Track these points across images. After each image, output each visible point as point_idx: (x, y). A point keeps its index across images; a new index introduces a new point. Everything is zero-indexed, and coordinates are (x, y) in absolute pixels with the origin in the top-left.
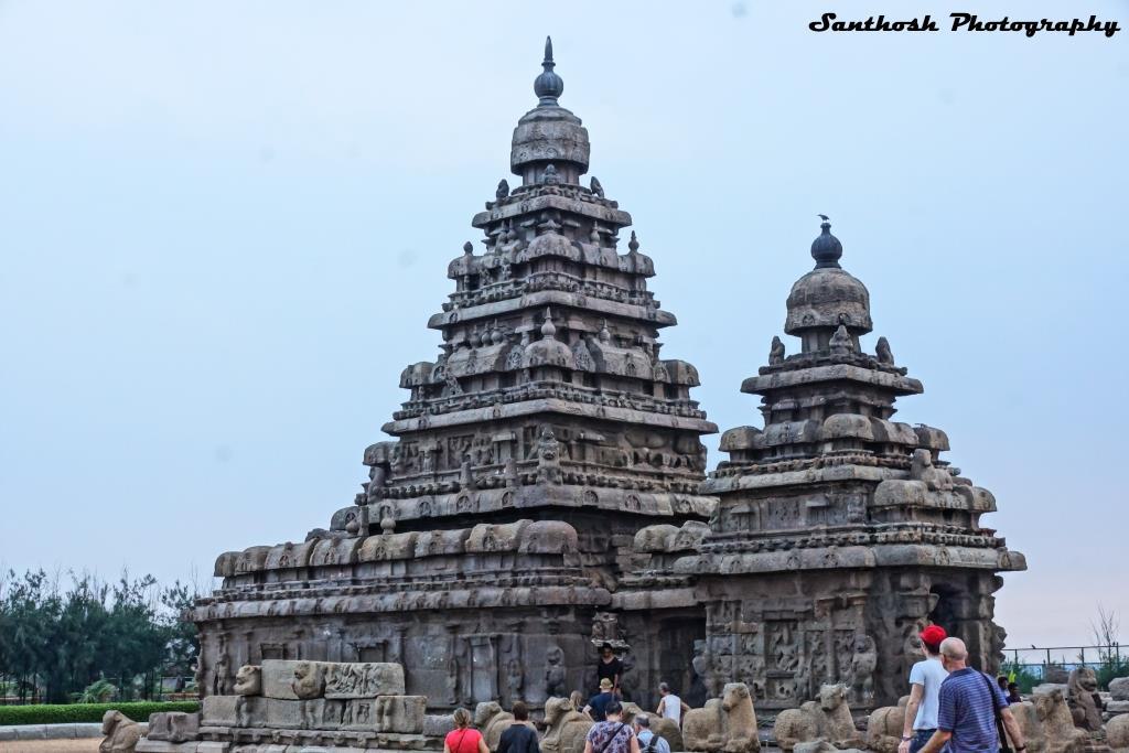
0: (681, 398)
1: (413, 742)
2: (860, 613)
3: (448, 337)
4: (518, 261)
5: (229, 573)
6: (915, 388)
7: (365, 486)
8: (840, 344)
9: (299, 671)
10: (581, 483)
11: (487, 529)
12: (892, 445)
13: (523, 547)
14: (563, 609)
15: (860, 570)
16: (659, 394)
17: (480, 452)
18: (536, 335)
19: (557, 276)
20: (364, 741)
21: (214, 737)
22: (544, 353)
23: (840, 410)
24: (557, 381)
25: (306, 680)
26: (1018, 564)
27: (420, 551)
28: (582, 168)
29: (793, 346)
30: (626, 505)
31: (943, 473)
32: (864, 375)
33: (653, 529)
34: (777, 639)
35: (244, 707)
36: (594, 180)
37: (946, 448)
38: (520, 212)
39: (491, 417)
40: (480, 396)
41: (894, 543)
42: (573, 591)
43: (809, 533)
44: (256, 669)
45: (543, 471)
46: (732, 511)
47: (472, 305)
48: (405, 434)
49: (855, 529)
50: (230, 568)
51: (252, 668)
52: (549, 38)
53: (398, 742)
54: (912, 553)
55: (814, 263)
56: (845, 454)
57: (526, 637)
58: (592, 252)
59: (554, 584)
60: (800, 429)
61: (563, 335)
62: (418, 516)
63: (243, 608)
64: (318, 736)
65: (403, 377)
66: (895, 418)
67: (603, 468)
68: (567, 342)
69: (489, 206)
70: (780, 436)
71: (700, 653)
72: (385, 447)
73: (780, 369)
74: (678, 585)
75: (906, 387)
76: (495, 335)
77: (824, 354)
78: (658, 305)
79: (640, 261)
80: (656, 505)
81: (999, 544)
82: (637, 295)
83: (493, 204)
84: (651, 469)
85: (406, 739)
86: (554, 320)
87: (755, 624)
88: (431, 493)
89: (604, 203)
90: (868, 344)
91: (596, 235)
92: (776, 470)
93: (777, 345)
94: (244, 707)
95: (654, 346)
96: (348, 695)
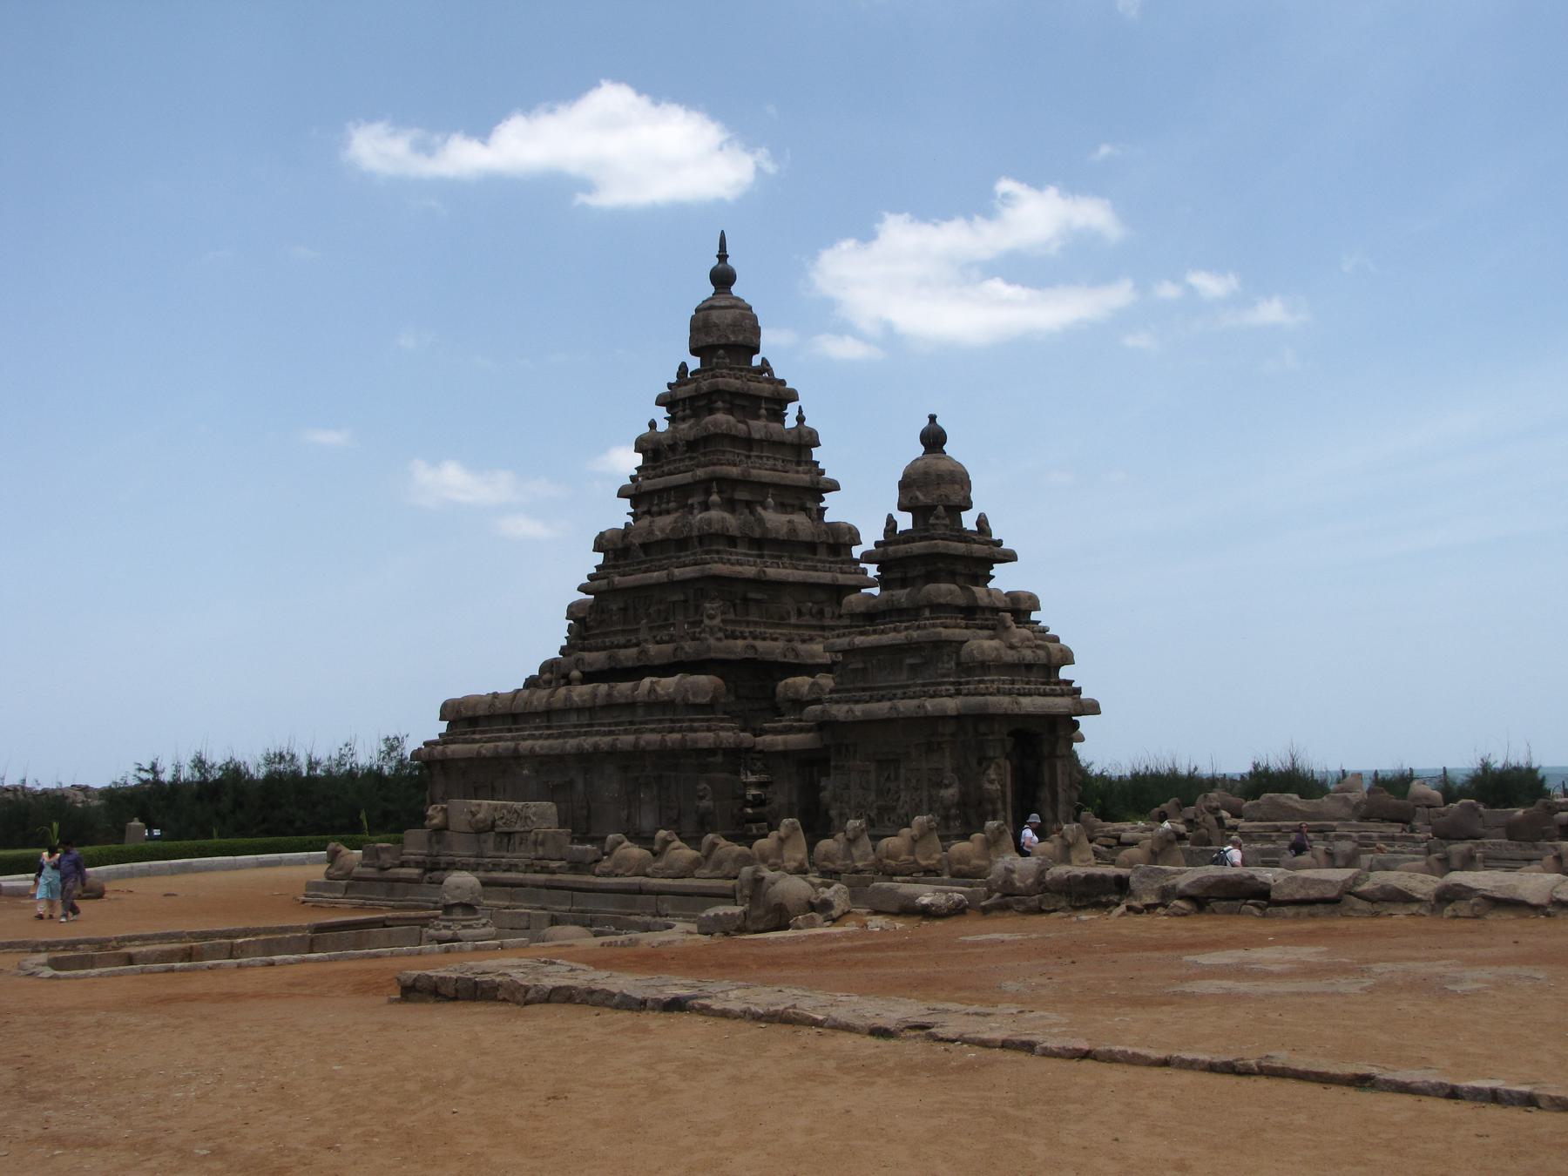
0: (844, 557)
1: (560, 867)
2: (948, 754)
4: (692, 438)
6: (1010, 557)
8: (938, 522)
9: (473, 809)
10: (745, 638)
11: (652, 683)
12: (984, 609)
14: (711, 752)
15: (943, 718)
16: (823, 554)
17: (659, 610)
18: (706, 507)
19: (724, 452)
20: (524, 867)
22: (709, 522)
23: (936, 580)
24: (722, 548)
25: (480, 816)
26: (1093, 708)
27: (599, 702)
28: (756, 350)
29: (905, 521)
30: (785, 656)
31: (1025, 632)
32: (960, 548)
33: (790, 680)
34: (886, 775)
35: (434, 839)
36: (764, 360)
37: (1037, 608)
38: (694, 394)
39: (666, 580)
41: (973, 695)
42: (718, 735)
43: (908, 686)
44: (442, 808)
45: (707, 629)
46: (851, 667)
49: (943, 683)
51: (439, 807)
52: (722, 232)
53: (548, 867)
54: (998, 703)
55: (922, 449)
56: (937, 619)
58: (759, 427)
59: (703, 731)
60: (901, 595)
61: (730, 505)
62: (606, 667)
63: (457, 749)
64: (489, 863)
66: (991, 585)
67: (765, 623)
68: (733, 511)
69: (670, 385)
70: (887, 601)
71: (824, 789)
74: (809, 730)
75: (1000, 557)
77: (927, 530)
78: (823, 472)
79: (804, 432)
80: (813, 656)
81: (1078, 691)
82: (803, 464)
83: (673, 384)
85: (554, 865)
86: (720, 492)
87: (867, 763)
88: (619, 647)
89: (772, 380)
90: (969, 521)
91: (763, 412)
92: (883, 632)
93: (891, 523)
94: (434, 839)
95: (818, 510)
96: (511, 830)
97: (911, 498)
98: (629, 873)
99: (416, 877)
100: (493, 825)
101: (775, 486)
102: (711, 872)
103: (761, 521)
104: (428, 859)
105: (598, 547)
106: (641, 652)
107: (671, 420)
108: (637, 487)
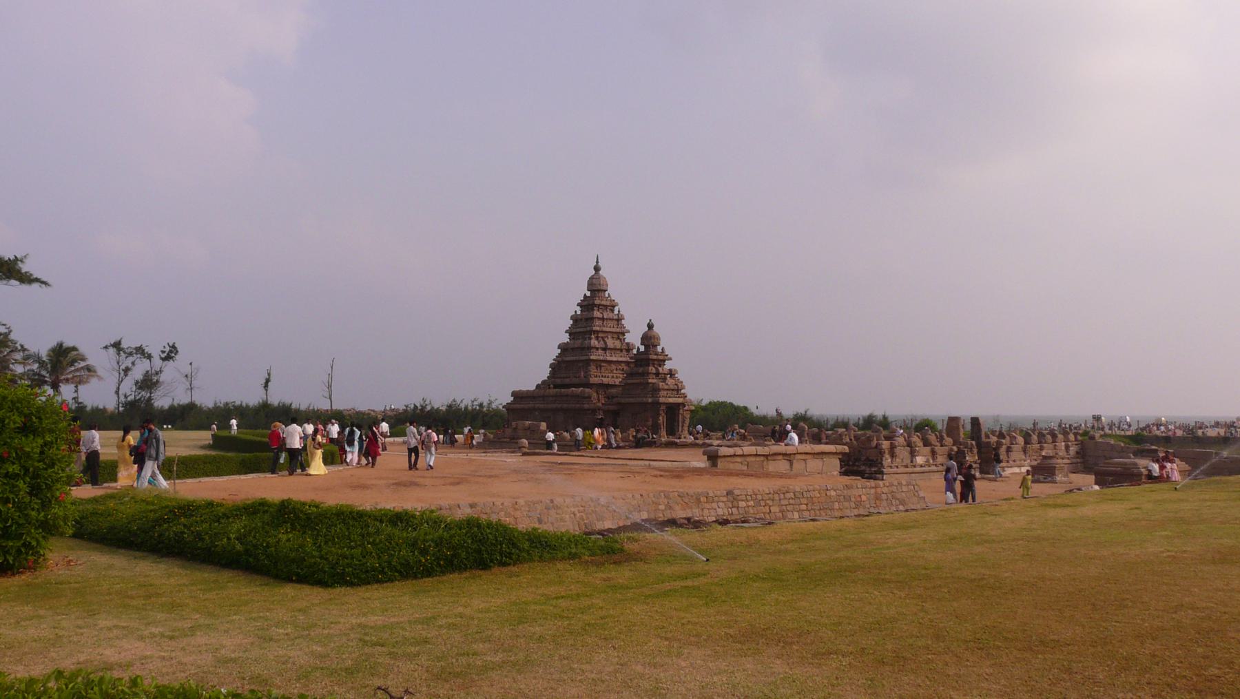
3: (570, 335)
6: (670, 359)
12: (661, 374)
14: (589, 410)
15: (648, 403)
32: (655, 357)
36: (609, 294)
48: (558, 362)
50: (514, 394)
61: (597, 338)
63: (518, 406)
66: (665, 366)
72: (553, 363)
81: (686, 397)
84: (621, 372)
88: (564, 378)
89: (611, 300)
90: (659, 349)
100: (529, 428)
101: (610, 332)
103: (605, 343)
105: (559, 348)
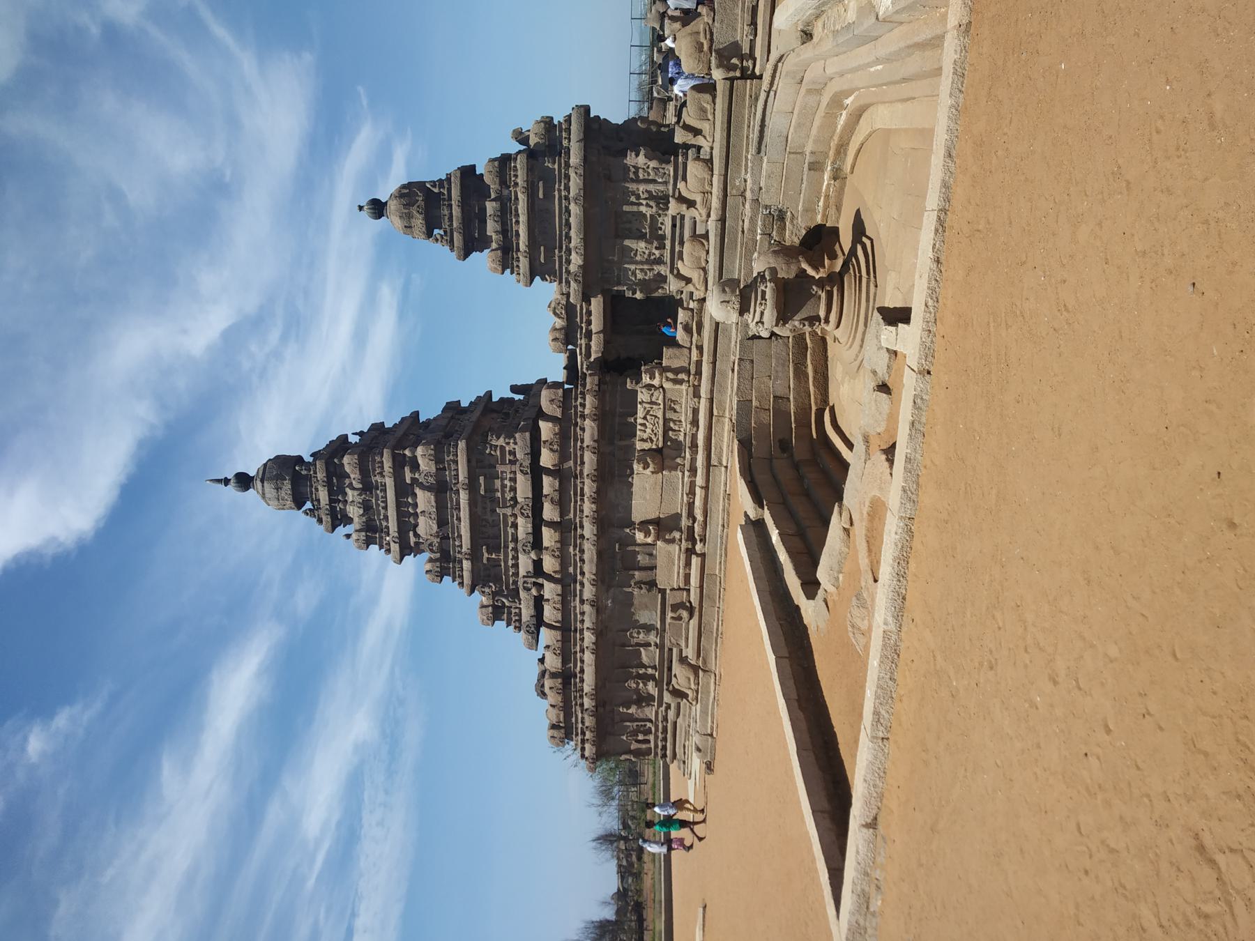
4: (360, 486)
5: (563, 731)
7: (507, 627)
13: (558, 413)
18: (415, 467)
20: (696, 400)
21: (687, 571)
36: (311, 456)
39: (467, 492)
40: (452, 508)
43: (560, 197)
45: (507, 441)
47: (387, 527)
57: (619, 410)
60: (490, 207)
65: (433, 580)
73: (452, 231)
74: (589, 313)
76: (410, 500)
88: (515, 550)
92: (517, 222)
96: (661, 422)
97: (418, 211)
98: (706, 243)
99: (700, 559)
102: (709, 120)
104: (684, 545)
106: (522, 514)
107: (348, 520)
108: (394, 541)
